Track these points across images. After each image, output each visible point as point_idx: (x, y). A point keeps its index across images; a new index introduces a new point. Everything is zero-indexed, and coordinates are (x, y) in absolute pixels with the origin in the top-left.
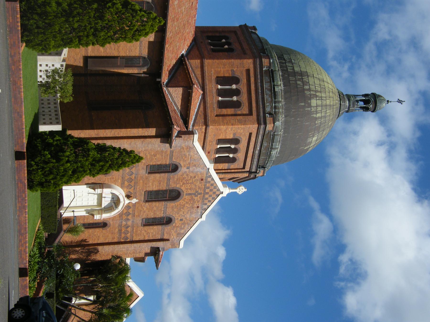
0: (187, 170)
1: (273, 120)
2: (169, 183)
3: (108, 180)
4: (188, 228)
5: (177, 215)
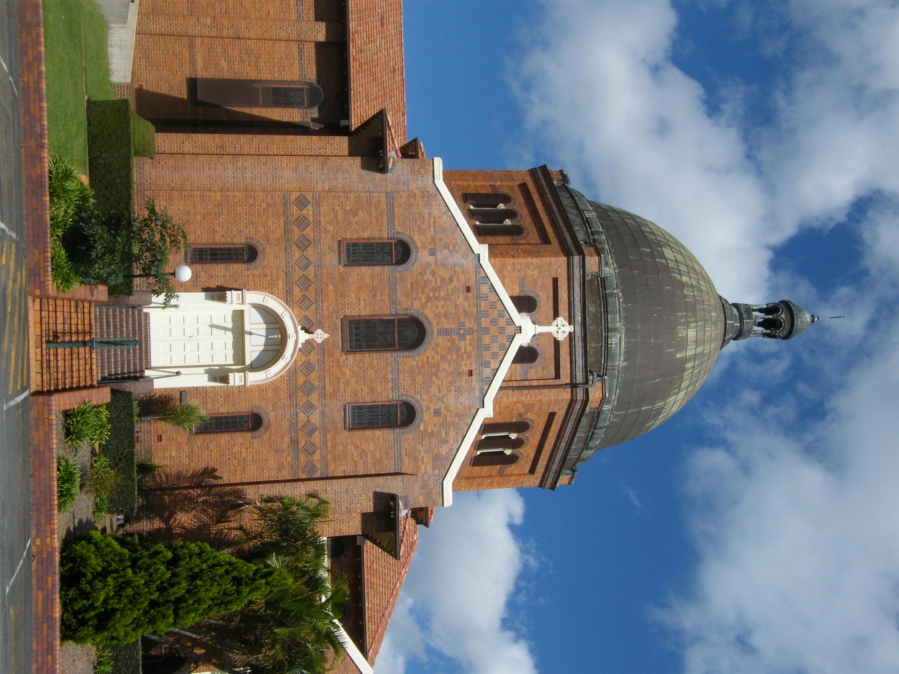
0: (431, 259)
1: (595, 251)
2: (396, 297)
3: (254, 281)
4: (457, 441)
5: (425, 397)
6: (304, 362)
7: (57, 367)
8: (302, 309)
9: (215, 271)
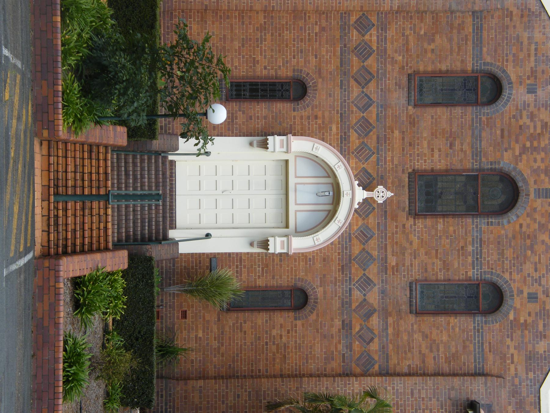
0: (529, 98)
2: (481, 146)
5: (516, 277)
6: (361, 227)
7: (66, 224)
8: (360, 161)
9: (254, 110)
